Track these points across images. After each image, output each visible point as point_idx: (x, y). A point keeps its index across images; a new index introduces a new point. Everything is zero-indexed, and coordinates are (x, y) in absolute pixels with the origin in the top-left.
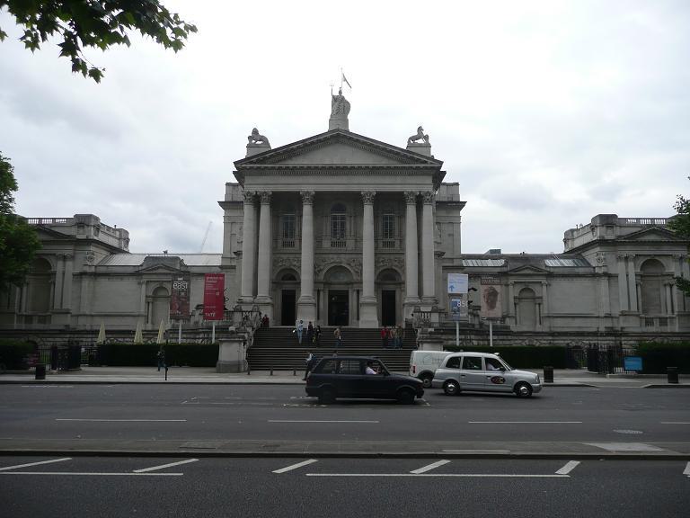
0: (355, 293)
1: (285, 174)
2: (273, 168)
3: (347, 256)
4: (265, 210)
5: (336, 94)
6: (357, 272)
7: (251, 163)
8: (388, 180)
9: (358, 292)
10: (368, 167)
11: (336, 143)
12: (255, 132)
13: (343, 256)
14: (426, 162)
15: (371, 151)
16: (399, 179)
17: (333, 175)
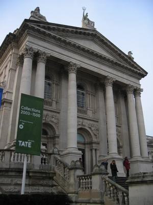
0: (94, 151)
1: (60, 46)
2: (54, 38)
3: (89, 122)
4: (41, 67)
5: (85, 15)
6: (95, 135)
7: (39, 26)
8: (120, 74)
9: (96, 150)
10: (112, 62)
11: (92, 40)
12: (38, 9)
13: (86, 121)
14: (139, 70)
15: (111, 54)
16: (125, 76)
17: (91, 59)
